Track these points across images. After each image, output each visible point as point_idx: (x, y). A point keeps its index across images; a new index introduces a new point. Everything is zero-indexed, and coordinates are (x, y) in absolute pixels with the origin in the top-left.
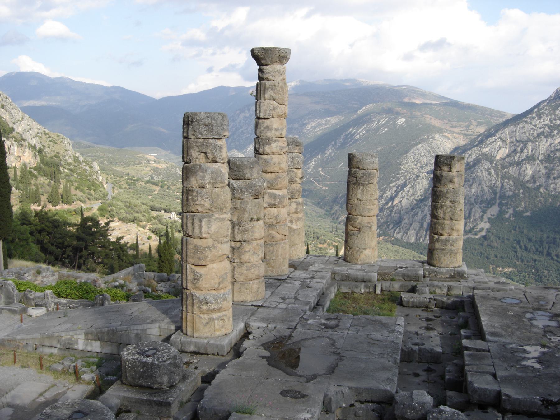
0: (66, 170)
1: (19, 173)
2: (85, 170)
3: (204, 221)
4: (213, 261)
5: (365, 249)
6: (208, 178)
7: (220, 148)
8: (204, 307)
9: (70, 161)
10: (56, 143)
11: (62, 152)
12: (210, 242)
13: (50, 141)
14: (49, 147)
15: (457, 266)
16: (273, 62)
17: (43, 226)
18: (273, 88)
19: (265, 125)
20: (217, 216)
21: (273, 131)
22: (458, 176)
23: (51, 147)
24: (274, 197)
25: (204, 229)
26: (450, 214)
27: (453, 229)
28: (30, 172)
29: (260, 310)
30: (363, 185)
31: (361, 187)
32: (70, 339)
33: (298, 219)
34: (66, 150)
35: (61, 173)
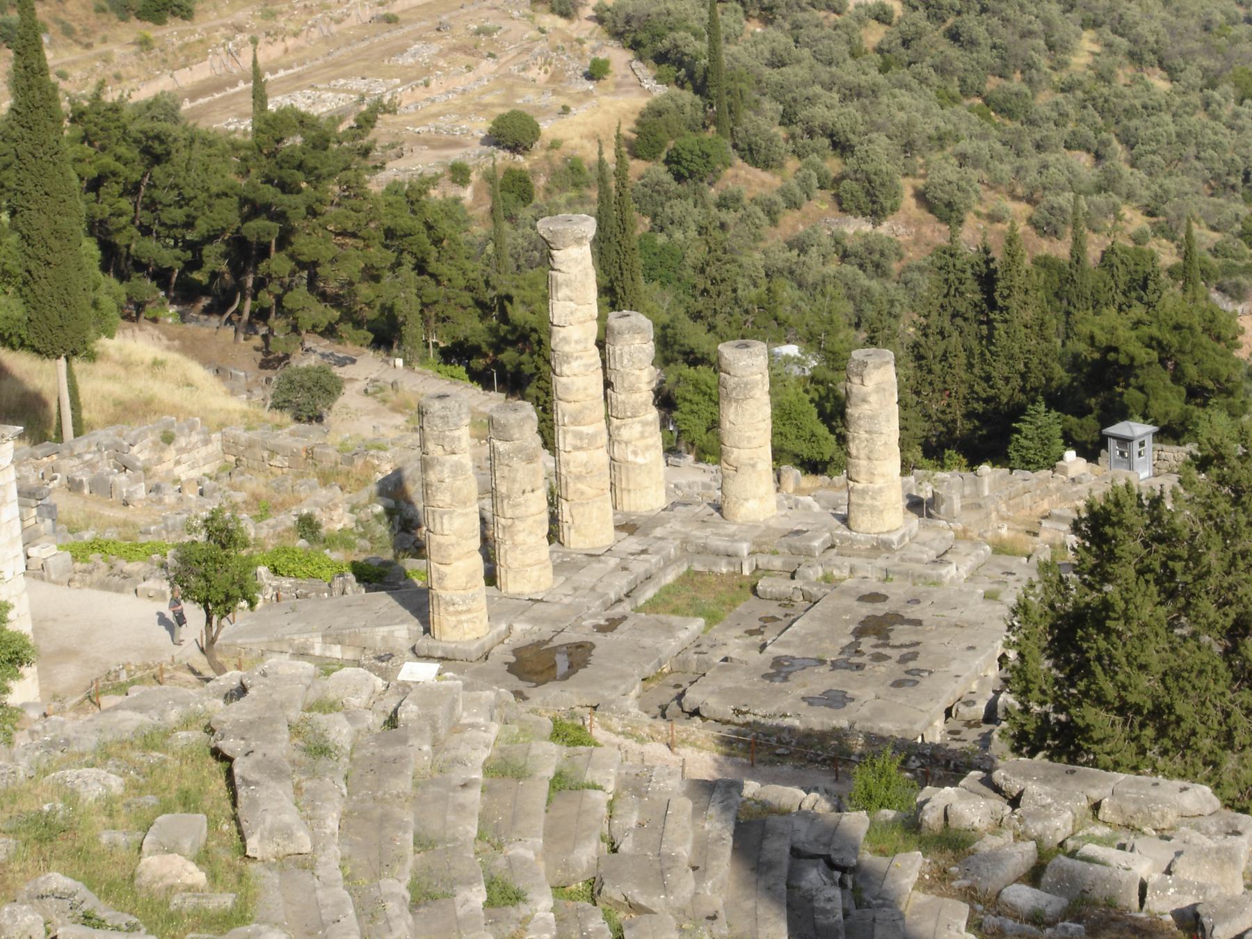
3: (446, 518)
4: (458, 559)
5: (746, 500)
6: (446, 473)
7: (459, 438)
8: (451, 609)
12: (453, 539)
15: (885, 530)
16: (566, 246)
17: (107, 160)
19: (561, 335)
20: (459, 511)
21: (573, 345)
22: (877, 392)
24: (579, 436)
25: (446, 526)
26: (866, 451)
27: (873, 474)
29: (537, 606)
30: (737, 401)
31: (734, 405)
32: (305, 643)
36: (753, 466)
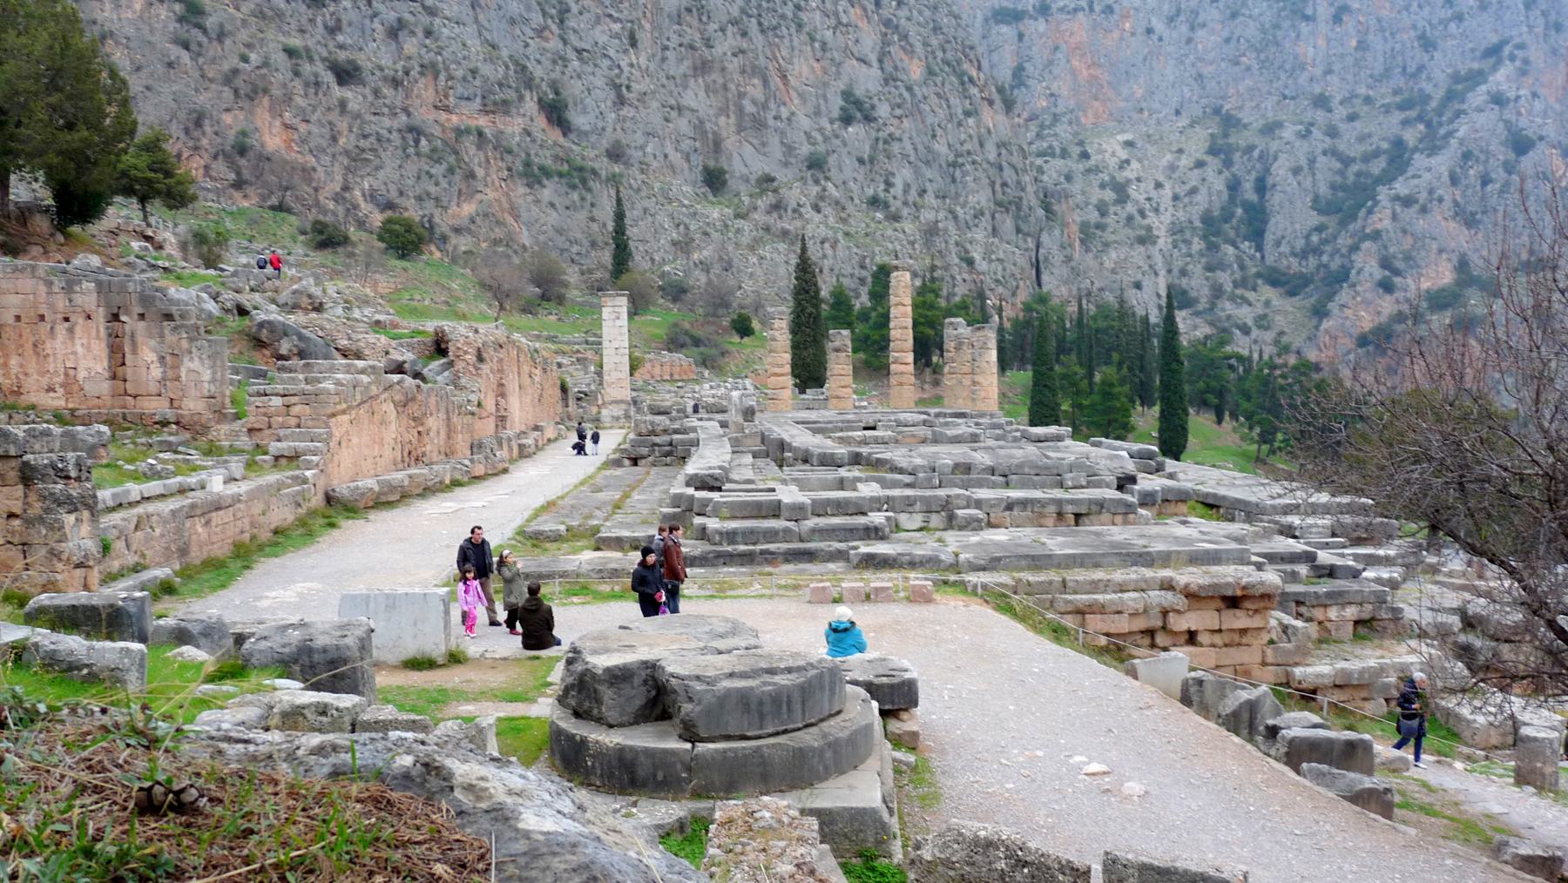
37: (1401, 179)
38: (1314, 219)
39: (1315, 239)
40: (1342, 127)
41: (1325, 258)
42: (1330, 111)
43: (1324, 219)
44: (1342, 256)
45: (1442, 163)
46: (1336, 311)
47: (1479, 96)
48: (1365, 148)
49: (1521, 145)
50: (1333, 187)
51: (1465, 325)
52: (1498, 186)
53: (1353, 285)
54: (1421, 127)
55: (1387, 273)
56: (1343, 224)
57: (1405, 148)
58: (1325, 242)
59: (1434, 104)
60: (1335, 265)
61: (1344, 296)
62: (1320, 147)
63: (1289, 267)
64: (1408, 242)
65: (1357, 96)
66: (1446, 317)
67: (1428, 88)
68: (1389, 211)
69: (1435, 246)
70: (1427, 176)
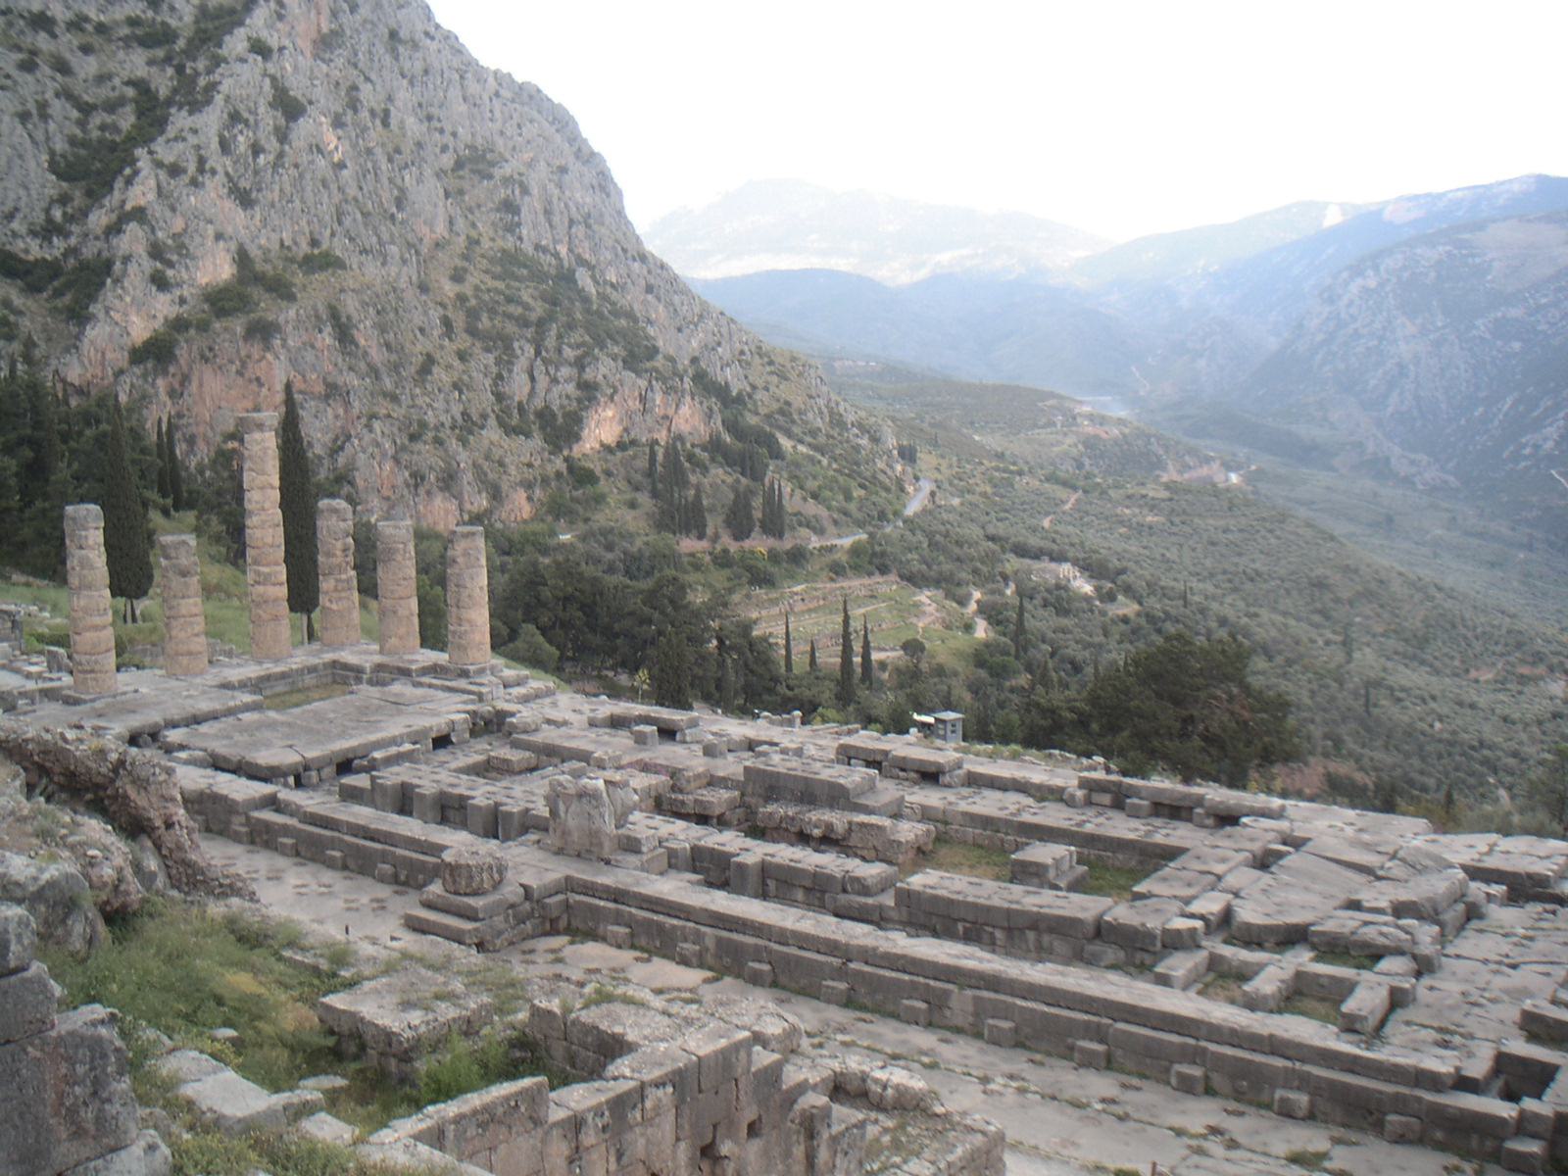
0: (802, 449)
1: (660, 457)
2: (857, 448)
7: (86, 537)
9: (819, 423)
10: (786, 379)
11: (798, 402)
12: (81, 614)
13: (772, 373)
14: (767, 389)
18: (250, 457)
23: (772, 389)
24: (258, 573)
28: (691, 457)
33: (340, 599)
34: (811, 397)
35: (777, 453)
36: (395, 612)
37: (161, 140)
38: (52, 186)
39: (57, 214)
40: (75, 60)
41: (73, 241)
42: (54, 36)
43: (64, 185)
44: (97, 238)
45: (211, 120)
46: (101, 315)
47: (236, 43)
48: (104, 92)
49: (290, 108)
50: (72, 141)
51: (262, 332)
52: (271, 158)
53: (117, 281)
54: (170, 71)
55: (158, 265)
56: (94, 196)
57: (156, 99)
58: (69, 218)
59: (181, 43)
60: (89, 252)
61: (109, 294)
62: (51, 87)
63: (27, 251)
64: (178, 224)
65: (87, 19)
66: (238, 325)
67: (173, 23)
68: (152, 183)
69: (210, 230)
70: (192, 140)
